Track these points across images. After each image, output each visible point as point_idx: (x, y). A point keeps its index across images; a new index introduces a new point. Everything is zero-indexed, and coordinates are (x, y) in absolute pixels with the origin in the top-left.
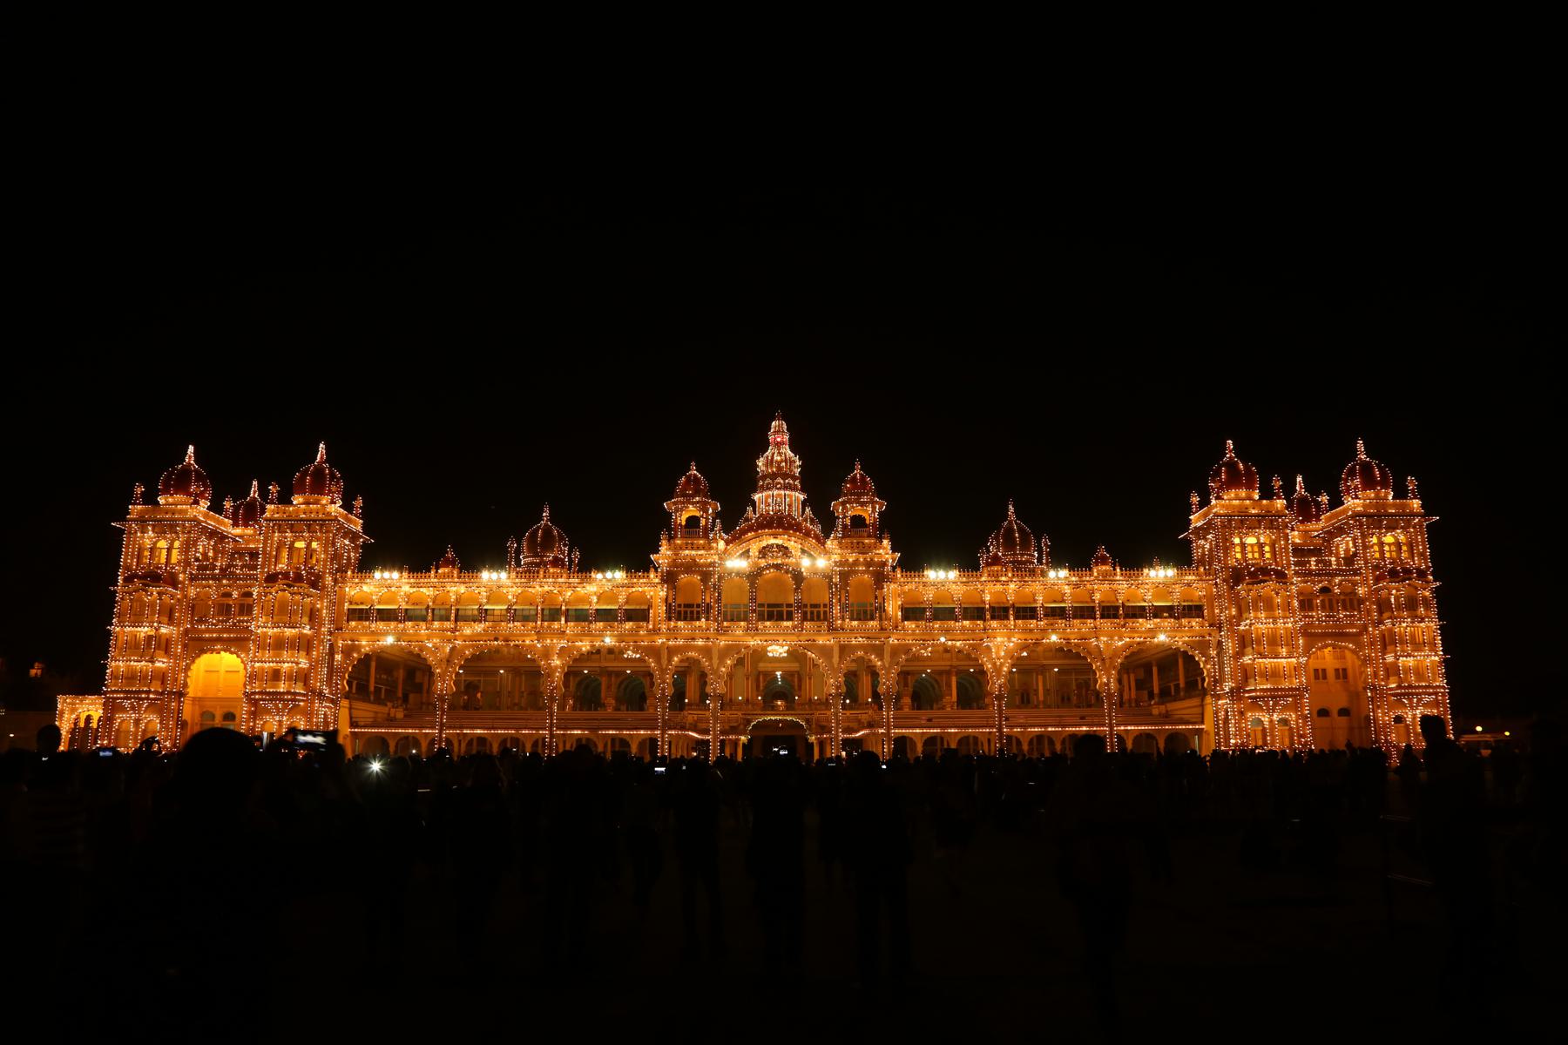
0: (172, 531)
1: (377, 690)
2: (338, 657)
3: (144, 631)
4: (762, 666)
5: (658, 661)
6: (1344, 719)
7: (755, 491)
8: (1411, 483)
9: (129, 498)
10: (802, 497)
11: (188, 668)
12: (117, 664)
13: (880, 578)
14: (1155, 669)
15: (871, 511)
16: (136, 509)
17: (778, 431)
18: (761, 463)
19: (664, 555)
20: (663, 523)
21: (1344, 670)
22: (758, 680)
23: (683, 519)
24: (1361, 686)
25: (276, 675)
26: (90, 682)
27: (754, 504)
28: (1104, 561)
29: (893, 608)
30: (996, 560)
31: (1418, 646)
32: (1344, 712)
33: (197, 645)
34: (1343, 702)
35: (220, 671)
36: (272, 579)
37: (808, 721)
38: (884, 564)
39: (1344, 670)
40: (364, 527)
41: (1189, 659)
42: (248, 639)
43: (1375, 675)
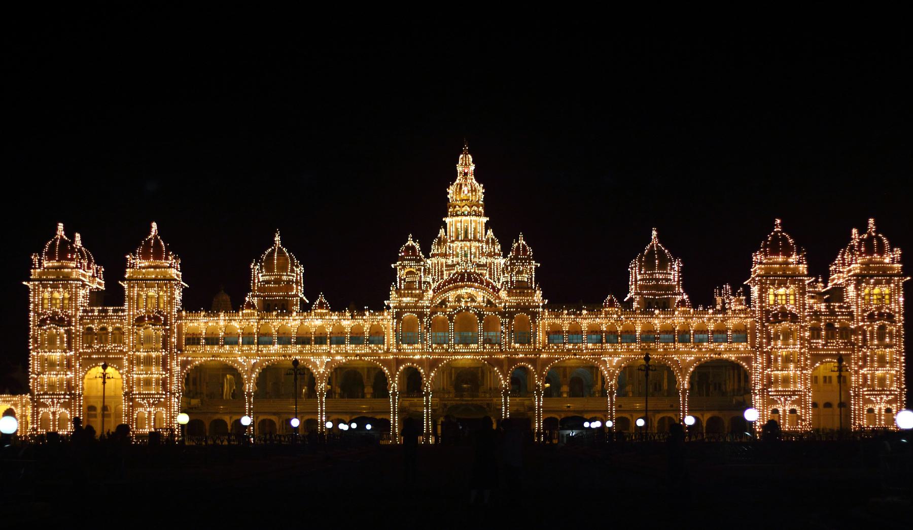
3: (57, 355)
5: (389, 369)
7: (446, 216)
9: (30, 265)
10: (485, 220)
11: (83, 378)
13: (534, 315)
16: (35, 273)
17: (466, 165)
18: (451, 190)
19: (393, 300)
22: (451, 374)
25: (148, 383)
27: (445, 225)
29: (541, 336)
30: (612, 304)
31: (882, 362)
33: (89, 362)
35: (104, 382)
38: (538, 307)
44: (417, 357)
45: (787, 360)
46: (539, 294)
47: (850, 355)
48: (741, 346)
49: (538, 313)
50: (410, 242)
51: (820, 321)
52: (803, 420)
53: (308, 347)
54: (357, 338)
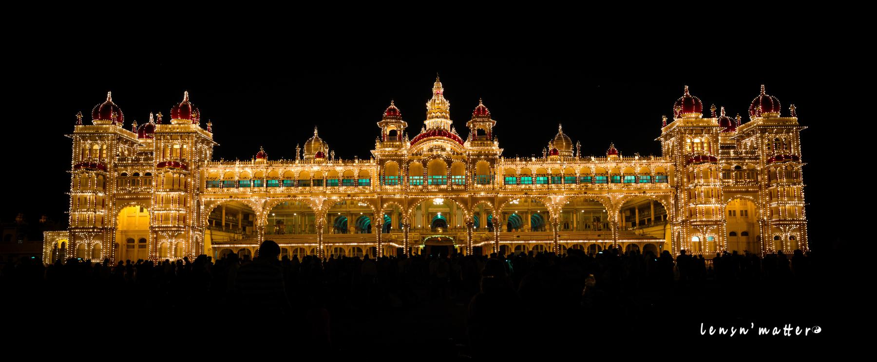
0: (102, 139)
1: (227, 225)
2: (202, 207)
3: (89, 195)
4: (430, 210)
5: (376, 207)
6: (744, 237)
8: (792, 108)
10: (450, 122)
11: (116, 215)
12: (76, 215)
14: (637, 211)
15: (489, 125)
17: (438, 88)
18: (429, 104)
19: (377, 152)
20: (377, 133)
21: (746, 211)
23: (387, 130)
24: (755, 221)
25: (167, 218)
26: (61, 223)
28: (613, 153)
29: (499, 179)
31: (791, 198)
32: (745, 234)
33: (121, 202)
34: (745, 229)
36: (161, 165)
37: (454, 237)
38: (496, 154)
39: (746, 211)
40: (214, 136)
41: (657, 204)
42: (150, 199)
43: (765, 214)
44: (398, 196)
45: (708, 195)
46: (496, 143)
47: (757, 192)
48: (663, 185)
49: (496, 159)
50: (392, 106)
51: (731, 164)
52: (721, 246)
53: (308, 188)
54: (348, 181)
